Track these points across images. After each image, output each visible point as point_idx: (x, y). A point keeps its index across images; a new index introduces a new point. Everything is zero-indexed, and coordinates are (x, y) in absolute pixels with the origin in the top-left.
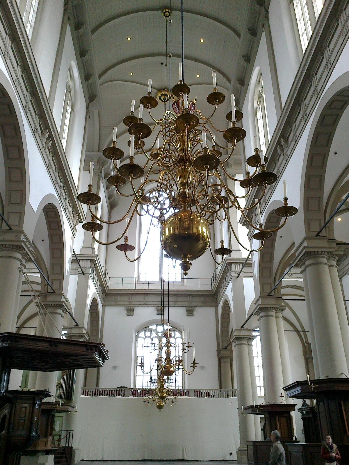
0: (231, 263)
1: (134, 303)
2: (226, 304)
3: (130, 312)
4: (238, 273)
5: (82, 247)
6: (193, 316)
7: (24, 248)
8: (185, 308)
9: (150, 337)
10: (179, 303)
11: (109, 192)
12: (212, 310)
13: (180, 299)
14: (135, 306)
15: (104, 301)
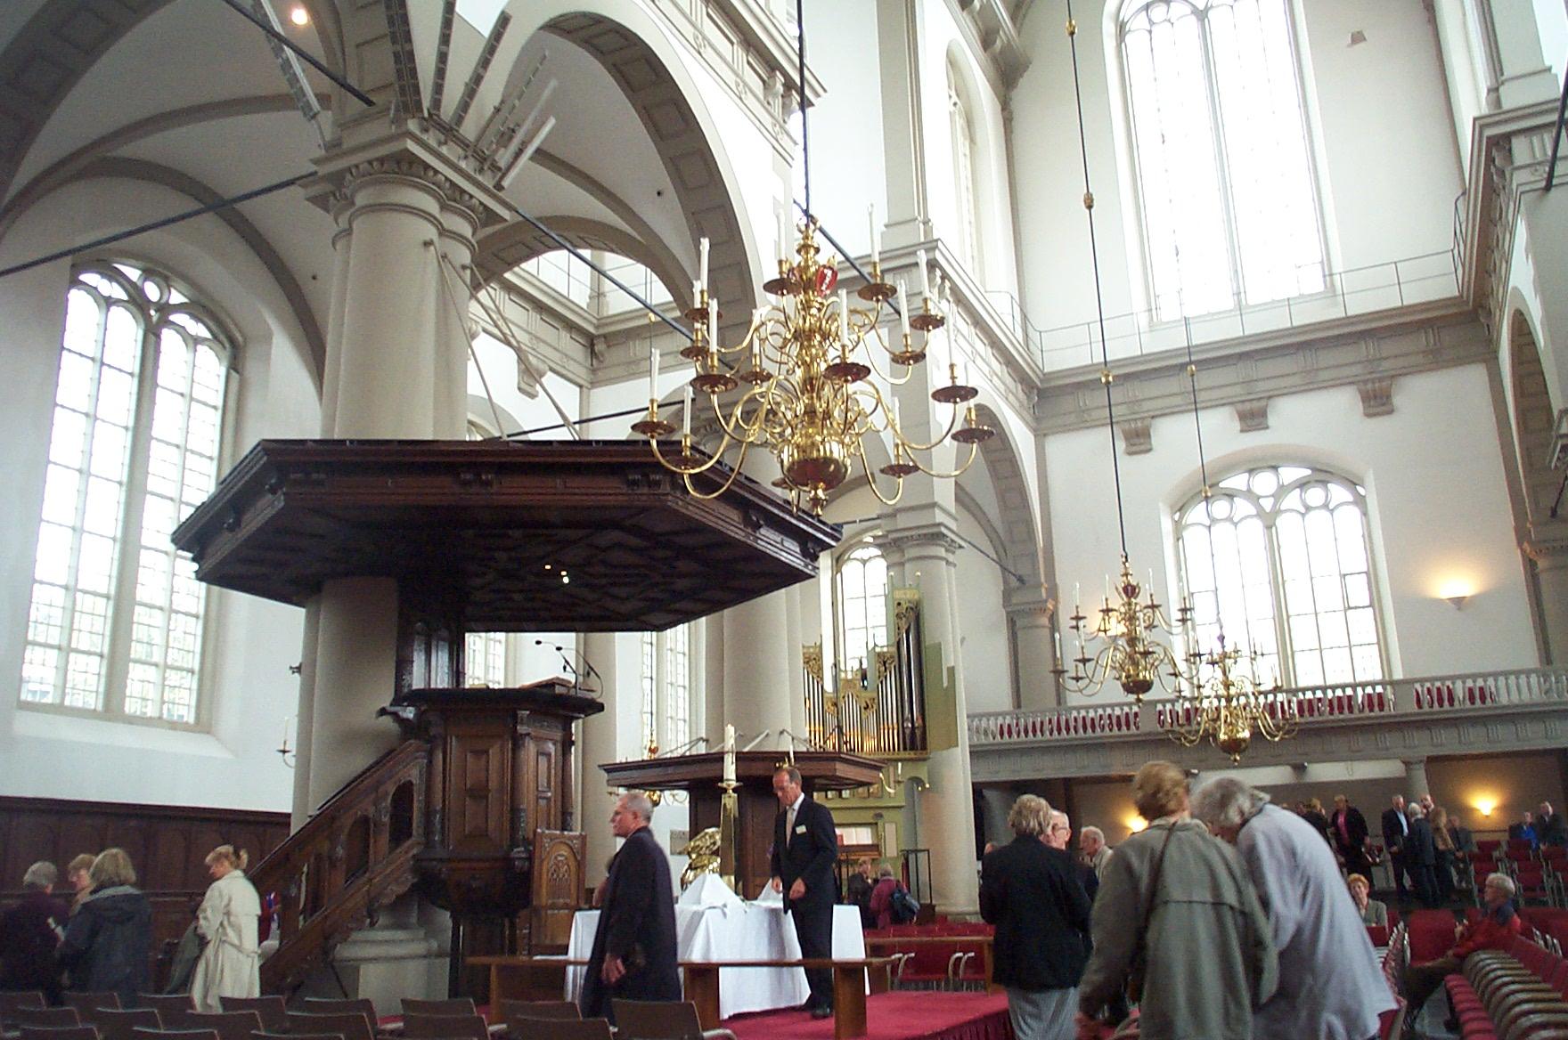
0: (1508, 137)
1: (1147, 405)
2: (1521, 325)
3: (1139, 440)
4: (1547, 169)
5: (886, 226)
6: (1391, 412)
7: (427, 167)
8: (1355, 387)
9: (1229, 519)
10: (1324, 375)
11: (976, 17)
12: (1475, 375)
13: (1327, 357)
14: (1153, 417)
15: (1037, 419)
